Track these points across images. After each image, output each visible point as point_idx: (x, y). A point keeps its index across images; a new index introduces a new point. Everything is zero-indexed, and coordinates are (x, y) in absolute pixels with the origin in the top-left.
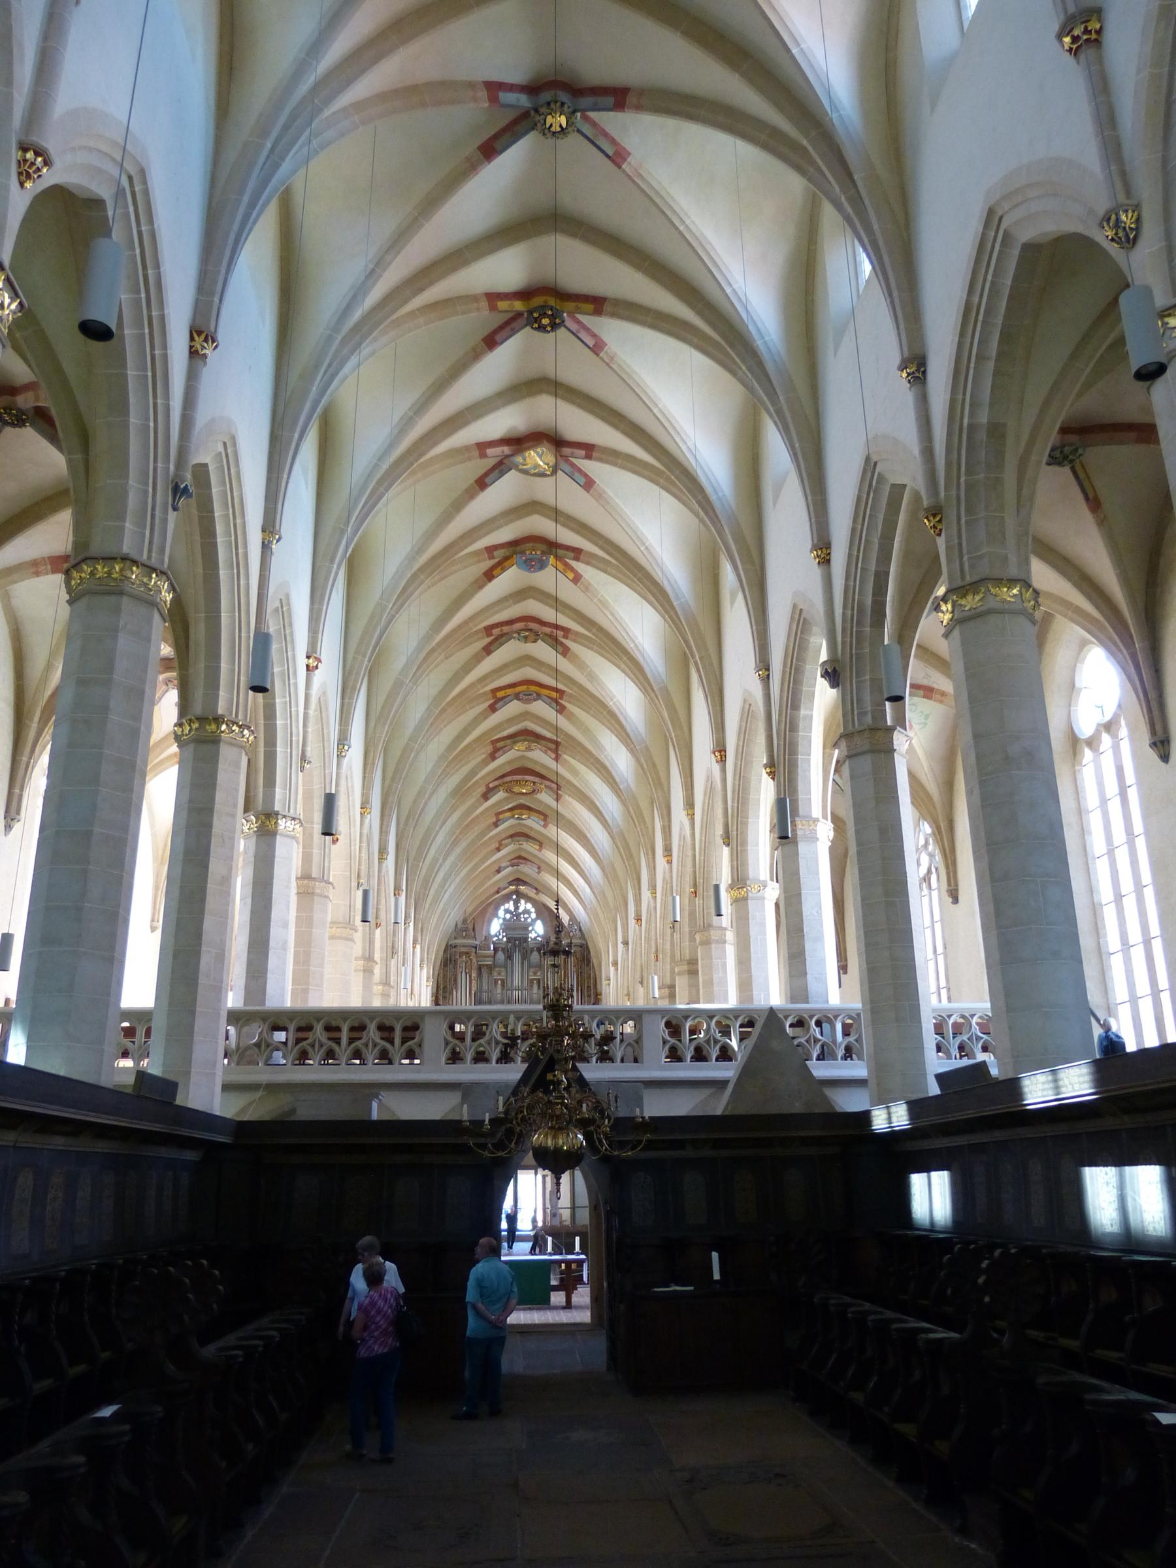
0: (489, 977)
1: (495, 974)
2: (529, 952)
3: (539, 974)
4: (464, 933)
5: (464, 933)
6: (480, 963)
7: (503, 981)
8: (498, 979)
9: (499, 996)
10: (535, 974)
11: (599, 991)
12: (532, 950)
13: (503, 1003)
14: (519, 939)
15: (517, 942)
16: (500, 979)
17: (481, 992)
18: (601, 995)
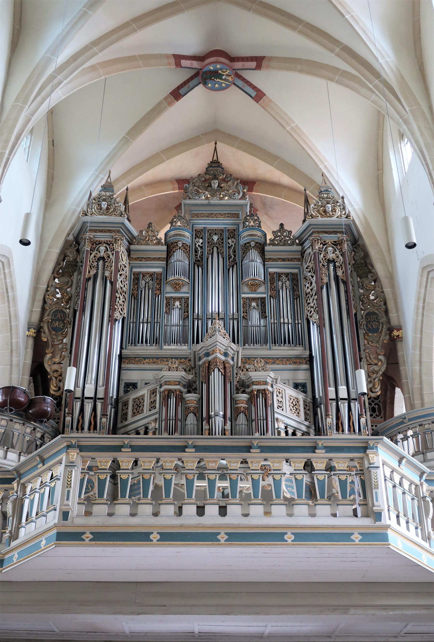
0: (155, 295)
1: (168, 288)
2: (240, 253)
3: (262, 289)
4: (104, 205)
5: (104, 205)
6: (135, 270)
7: (184, 301)
8: (175, 299)
9: (175, 329)
10: (254, 286)
11: (394, 322)
12: (246, 247)
13: (185, 342)
14: (220, 232)
15: (215, 238)
16: (180, 299)
17: (137, 323)
18: (399, 328)
